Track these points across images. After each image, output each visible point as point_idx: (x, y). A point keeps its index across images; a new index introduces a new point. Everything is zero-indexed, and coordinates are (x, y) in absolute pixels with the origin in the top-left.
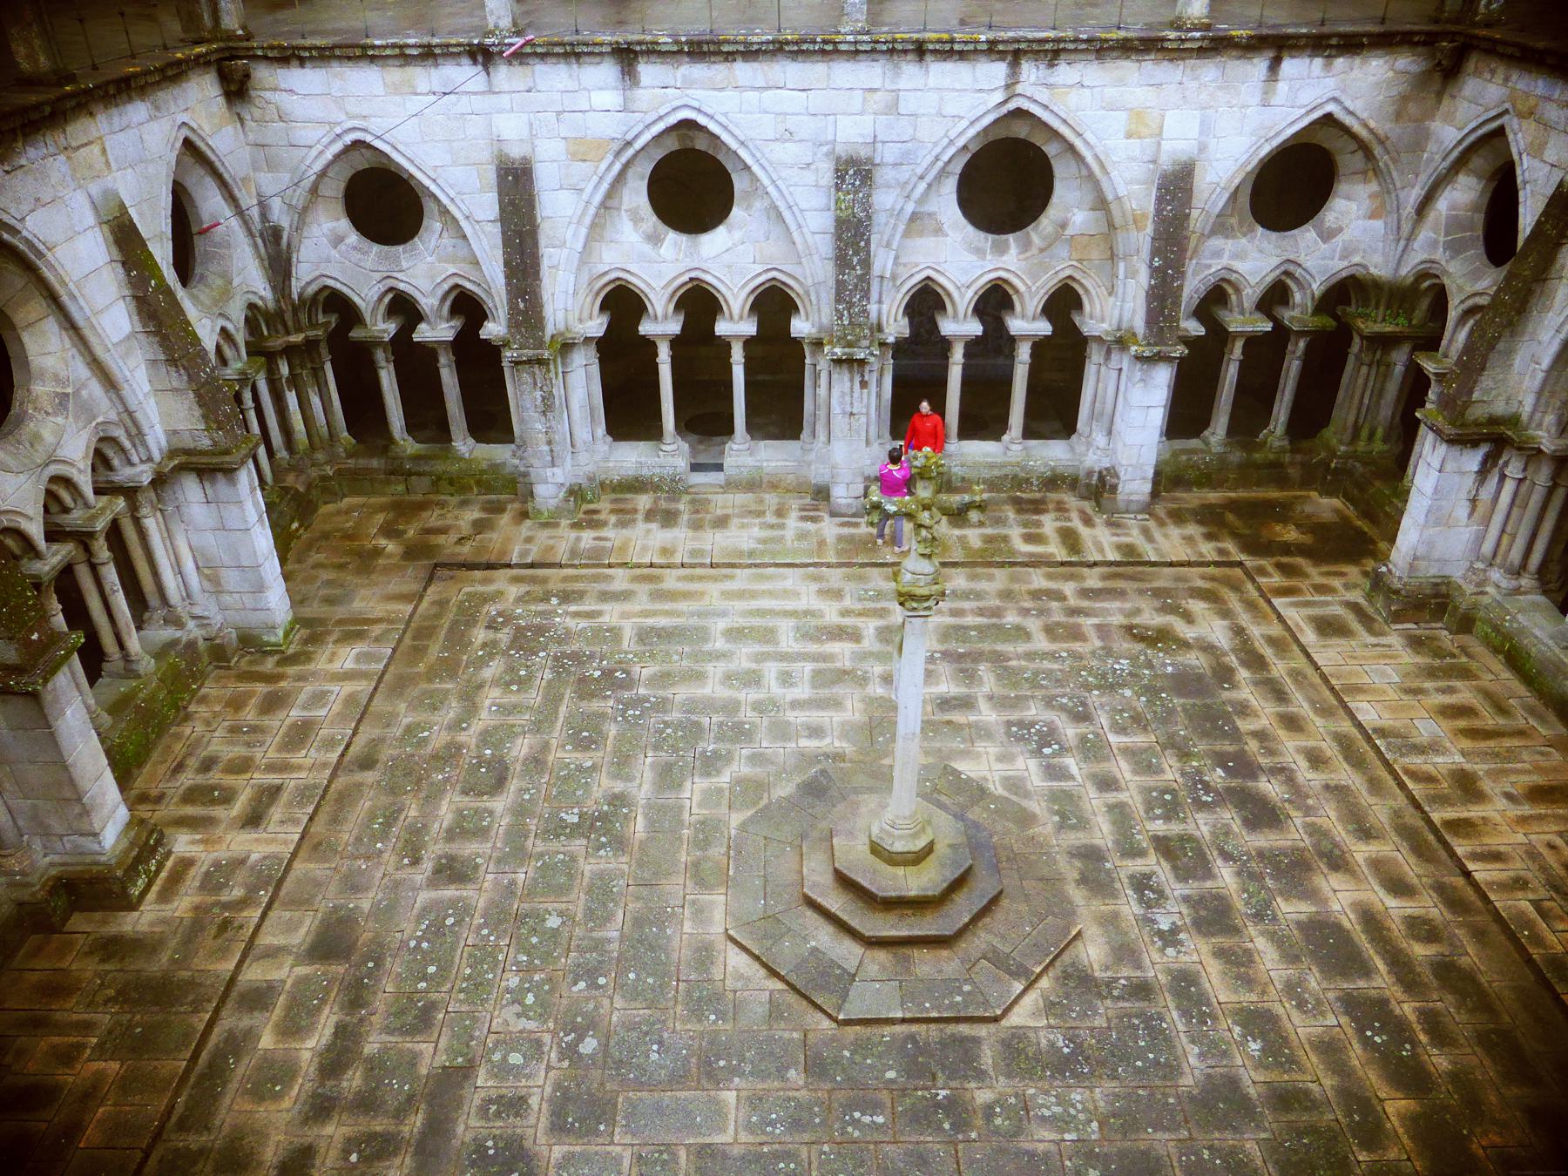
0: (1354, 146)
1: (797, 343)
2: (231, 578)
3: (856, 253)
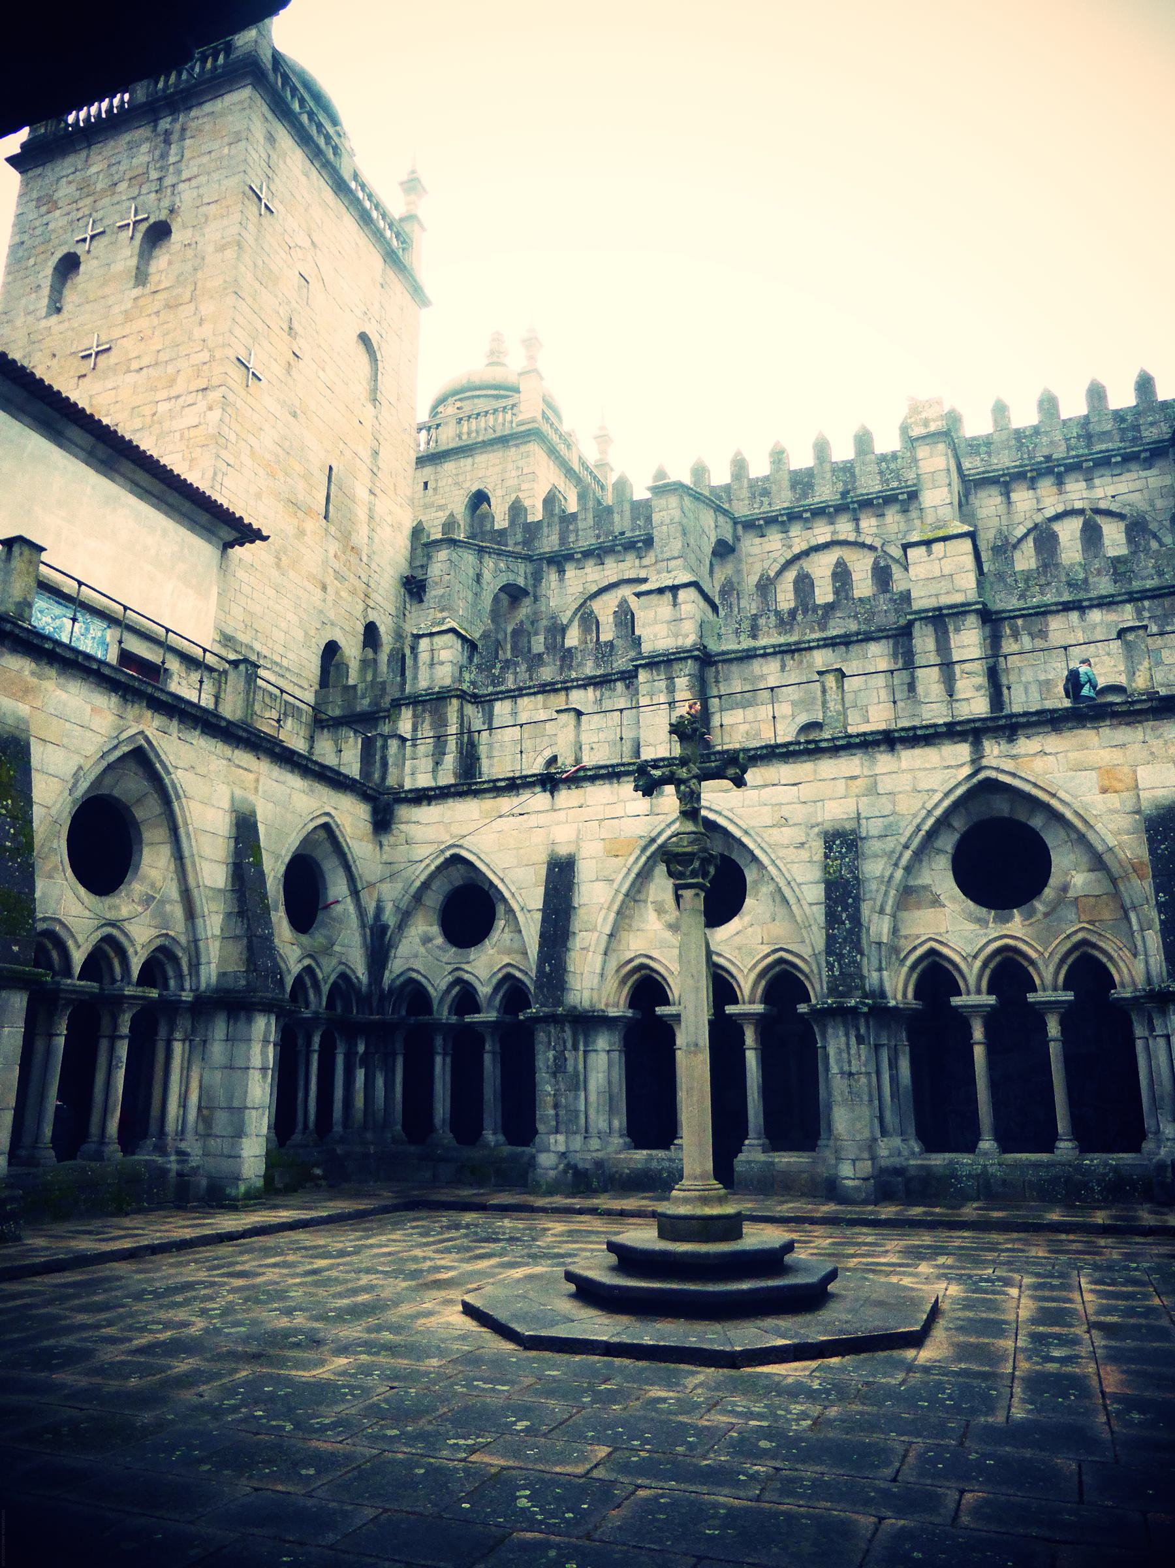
2: (221, 1119)
3: (845, 909)
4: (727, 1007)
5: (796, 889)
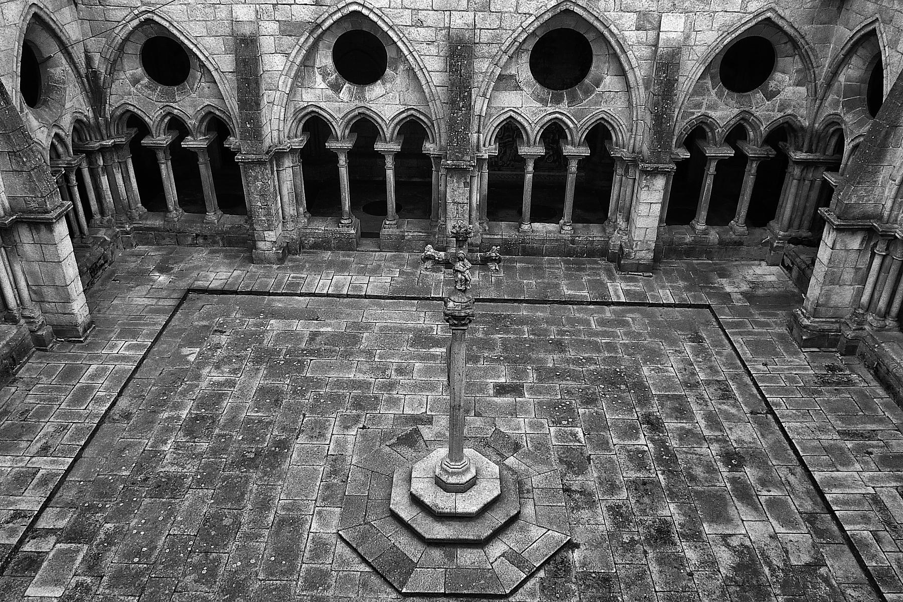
0: (786, 40)
1: (427, 157)
5: (426, 73)
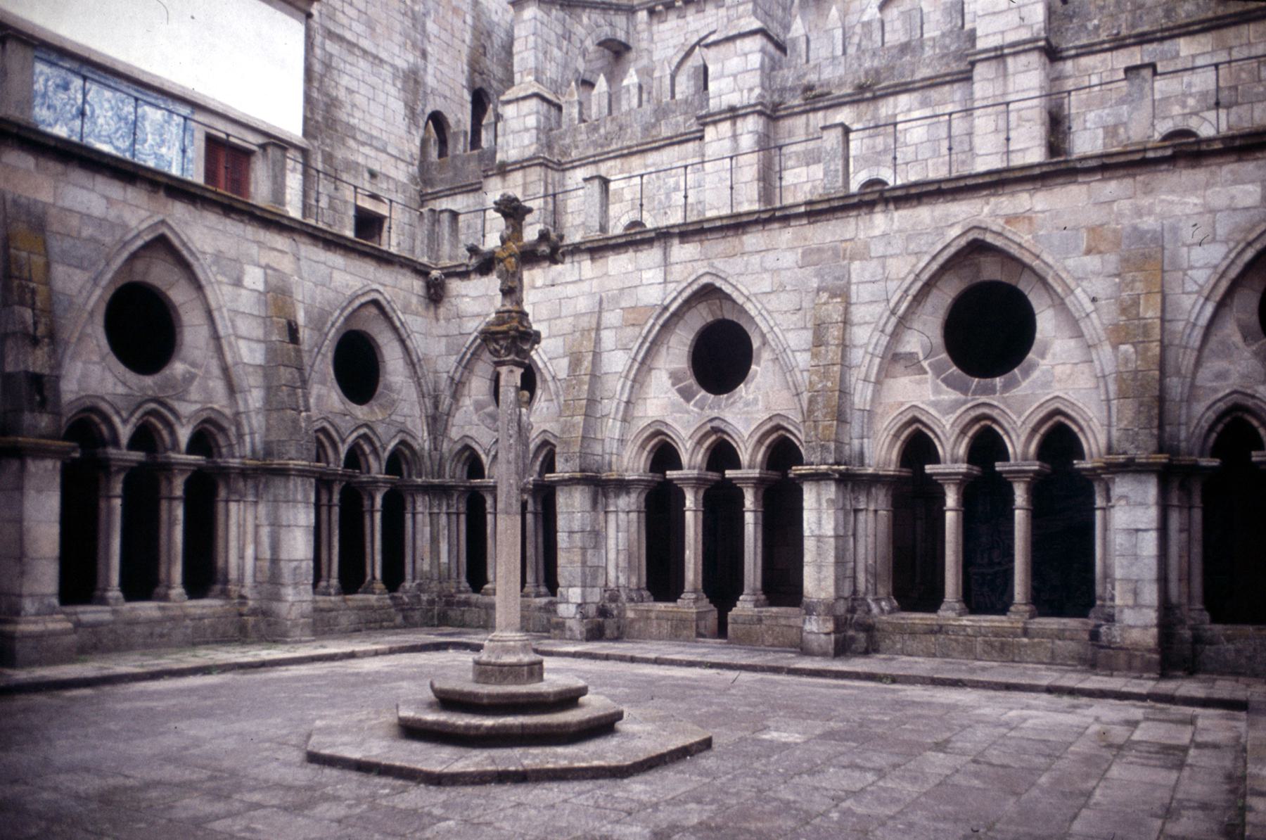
4: (997, 464)
